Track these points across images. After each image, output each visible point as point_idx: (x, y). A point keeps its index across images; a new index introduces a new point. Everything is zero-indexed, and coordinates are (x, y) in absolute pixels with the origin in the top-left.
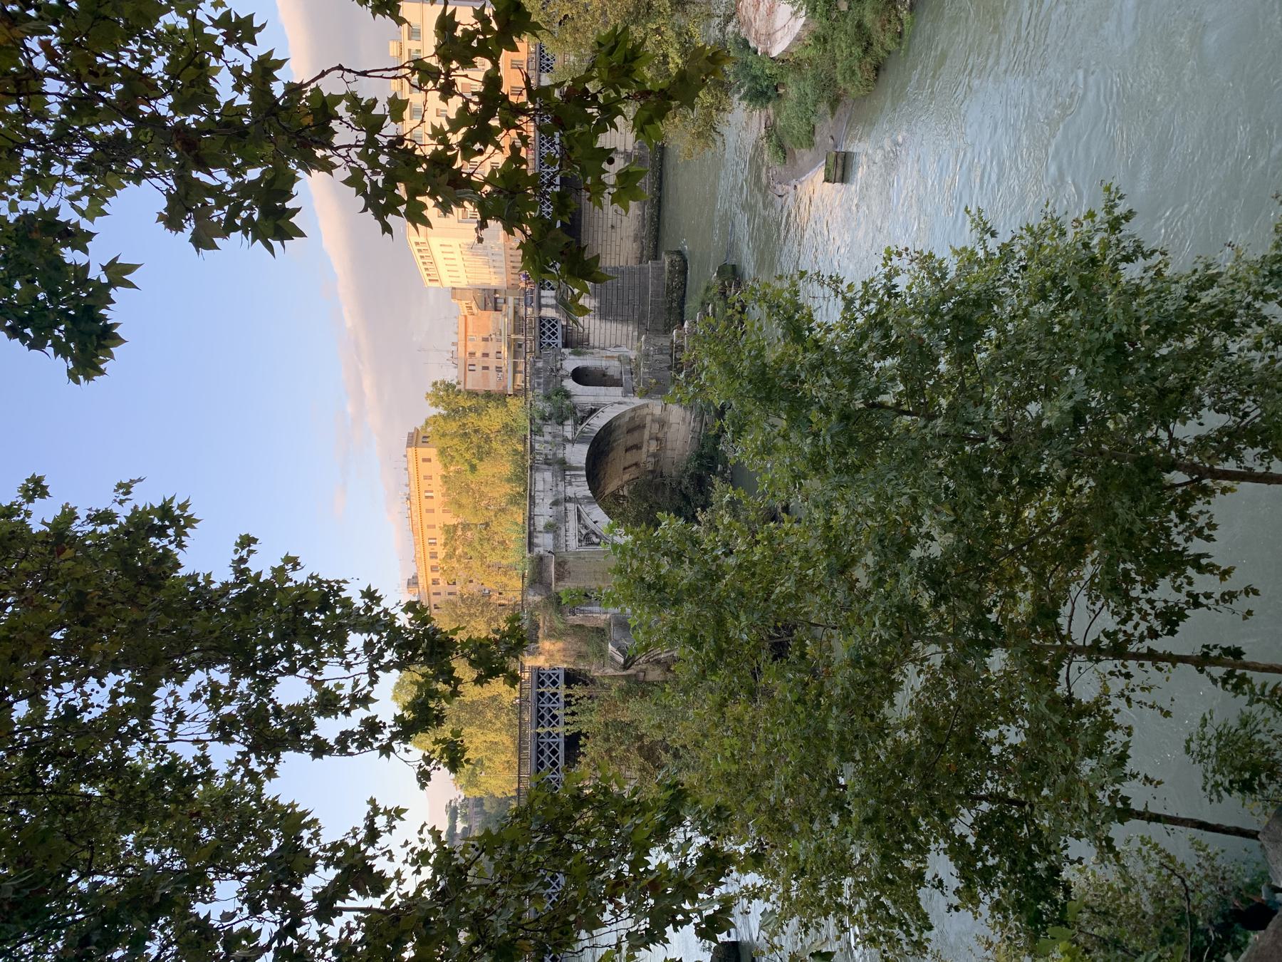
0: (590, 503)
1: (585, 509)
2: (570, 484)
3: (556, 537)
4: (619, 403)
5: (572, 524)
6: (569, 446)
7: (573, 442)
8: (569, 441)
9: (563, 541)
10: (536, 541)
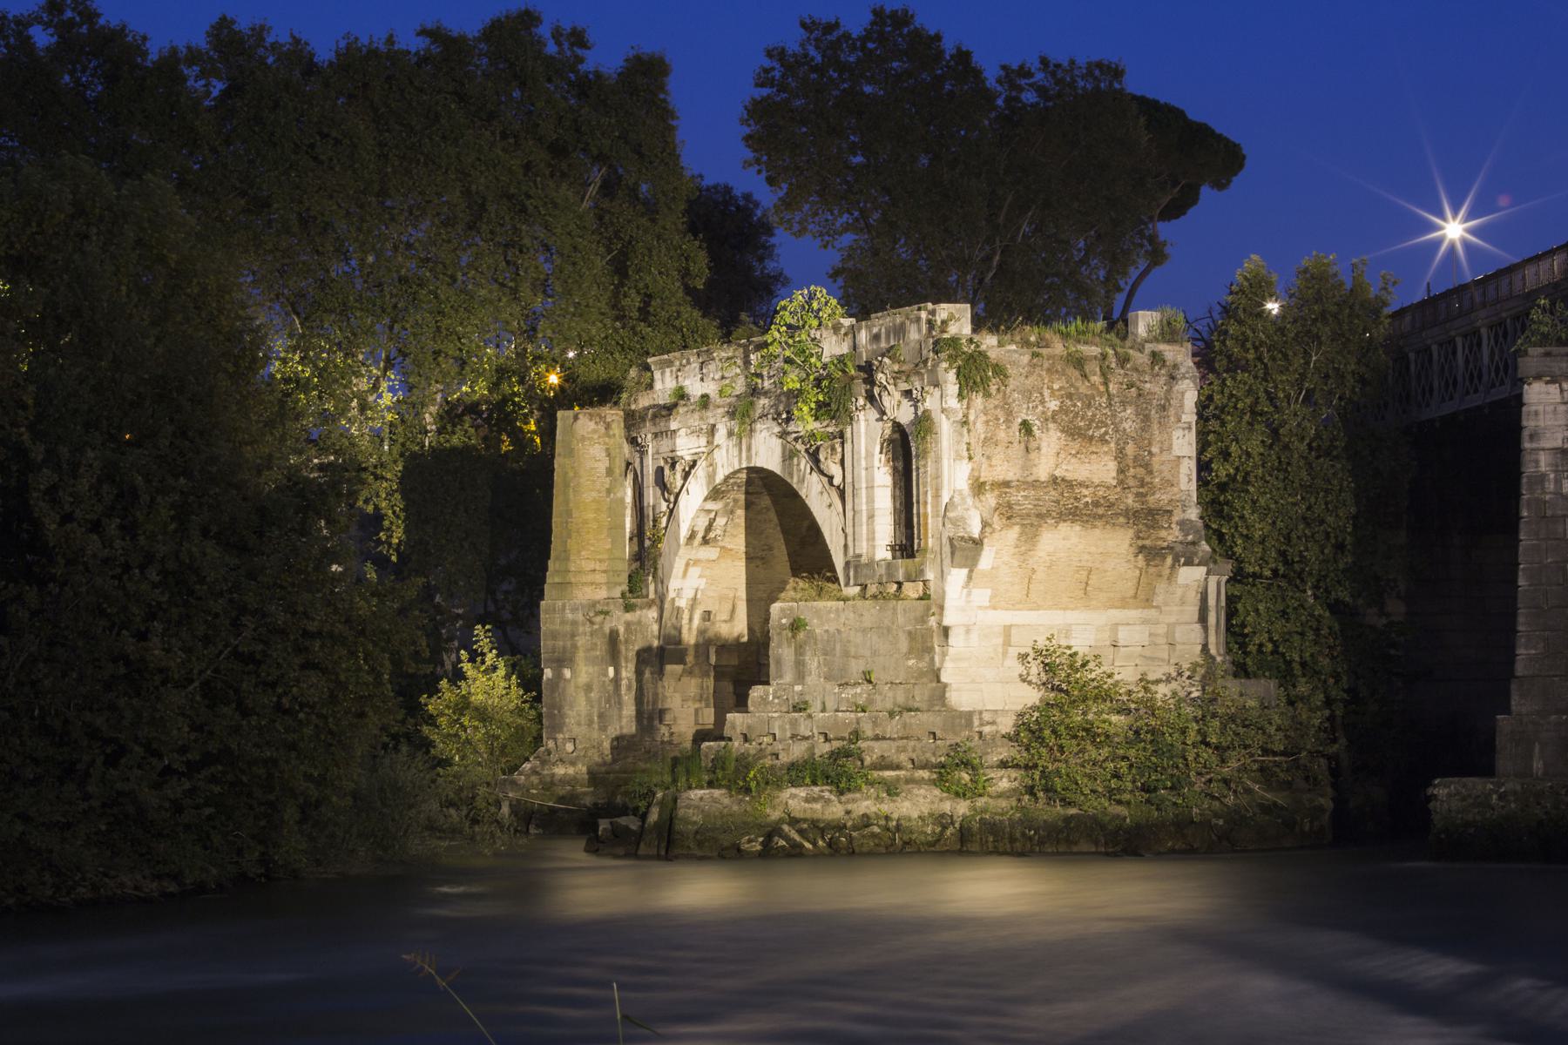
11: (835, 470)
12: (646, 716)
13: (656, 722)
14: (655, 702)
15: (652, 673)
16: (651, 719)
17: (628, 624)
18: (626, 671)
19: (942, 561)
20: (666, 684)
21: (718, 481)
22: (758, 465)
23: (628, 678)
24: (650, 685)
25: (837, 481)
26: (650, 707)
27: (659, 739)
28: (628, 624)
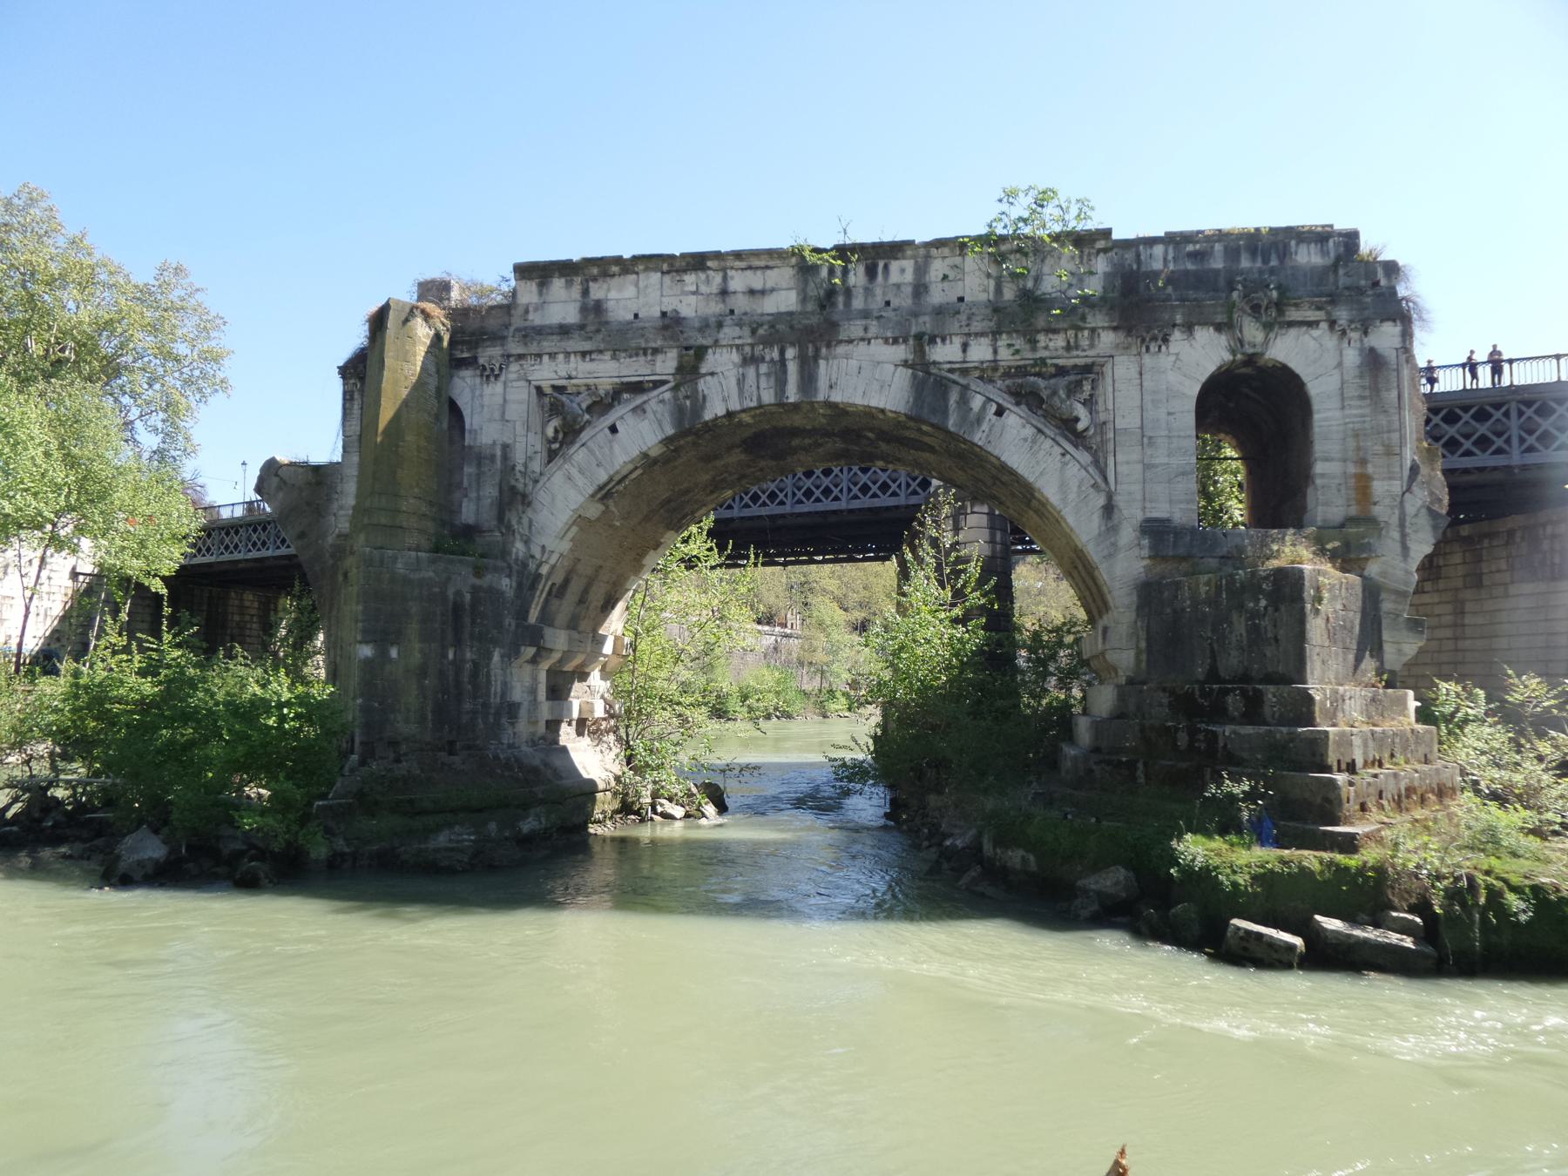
0: (679, 413)
1: (659, 404)
2: (750, 360)
3: (564, 331)
4: (1109, 509)
5: (606, 371)
6: (901, 352)
7: (920, 366)
8: (920, 351)
9: (548, 345)
10: (558, 284)
11: (1081, 411)
12: (492, 711)
13: (504, 720)
14: (503, 694)
15: (502, 656)
16: (498, 714)
17: (475, 590)
18: (471, 651)
19: (1404, 536)
20: (514, 671)
21: (708, 416)
22: (836, 397)
23: (473, 661)
24: (499, 672)
25: (1081, 426)
26: (498, 700)
27: (506, 742)
28: (475, 590)
